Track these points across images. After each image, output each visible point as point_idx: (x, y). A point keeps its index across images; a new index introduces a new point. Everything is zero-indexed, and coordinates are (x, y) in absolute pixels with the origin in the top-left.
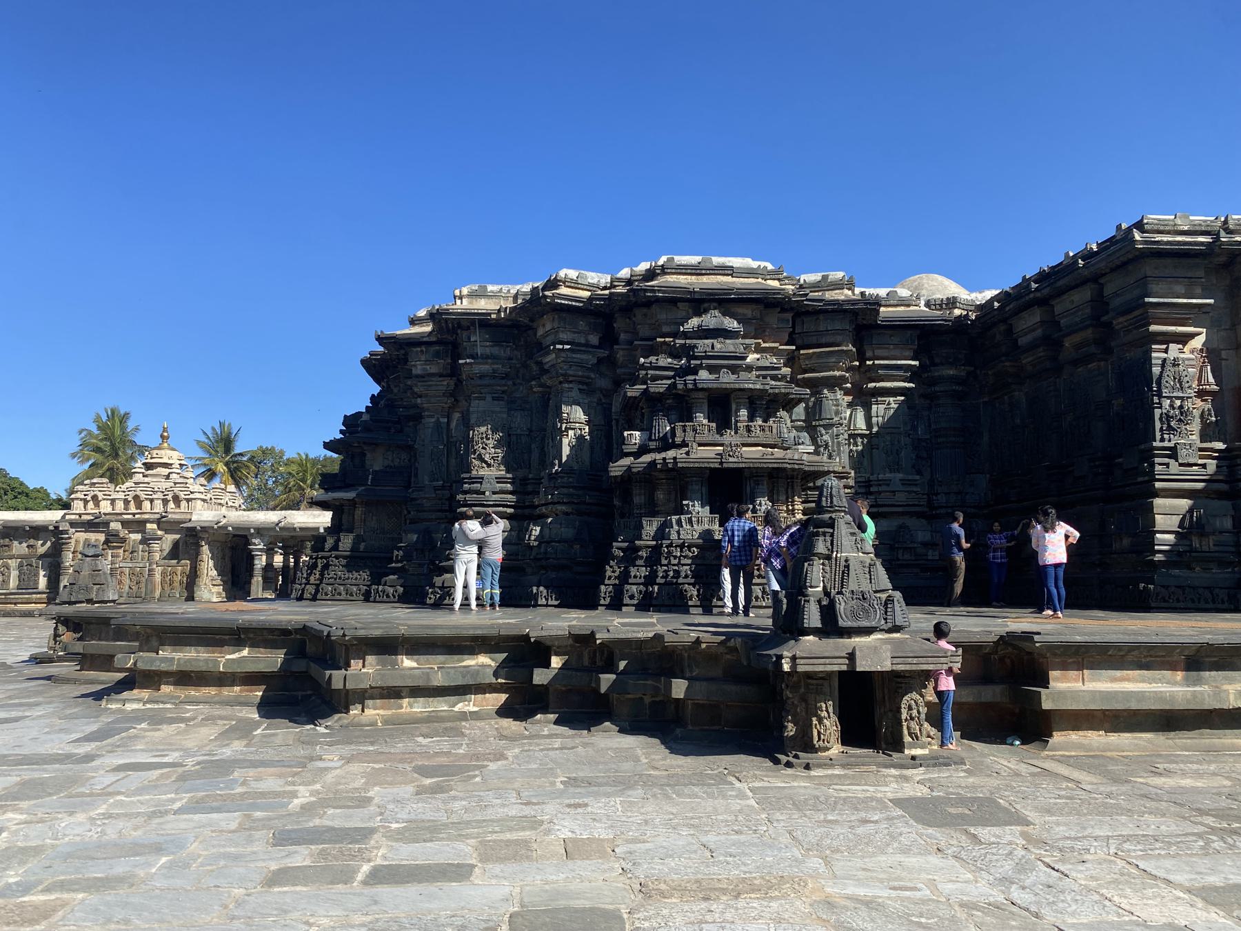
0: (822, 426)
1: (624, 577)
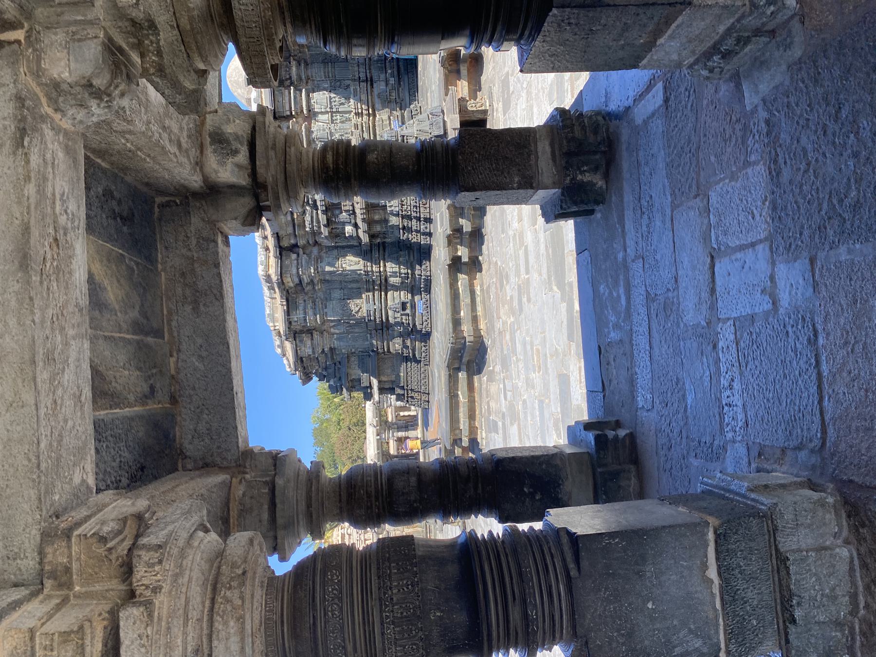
1: (417, 231)
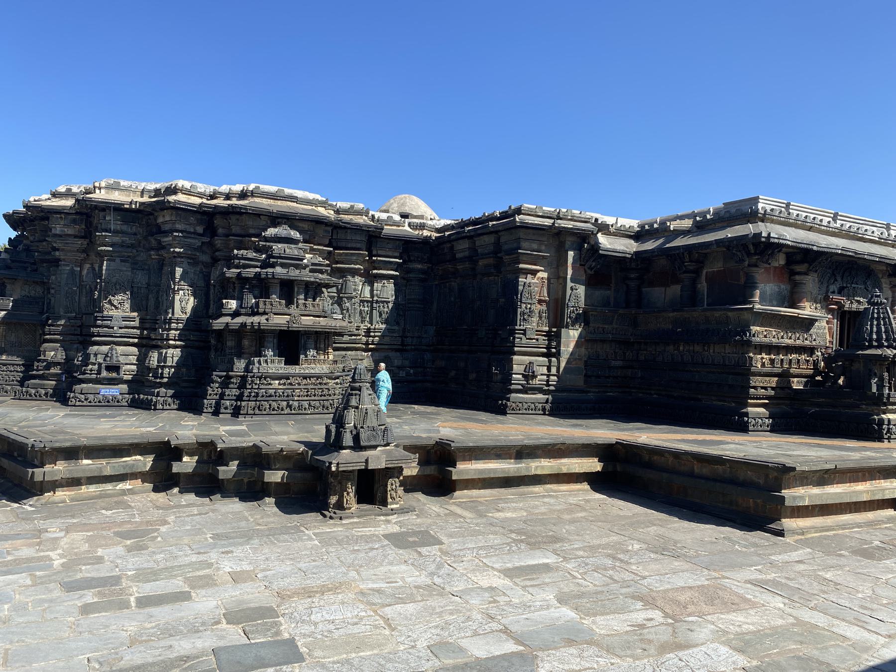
1: (222, 396)
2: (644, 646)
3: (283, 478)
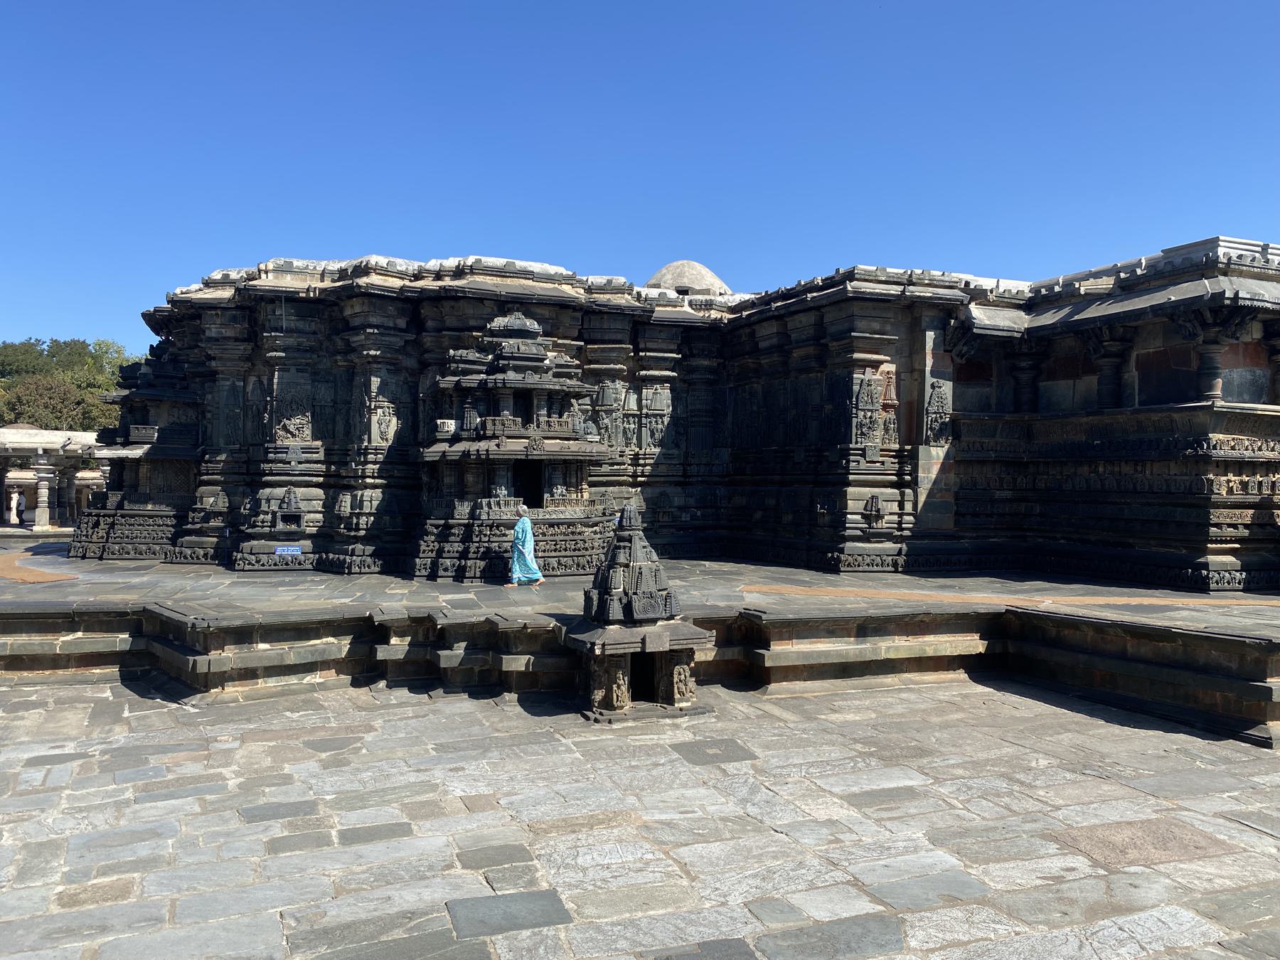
0: (605, 411)
1: (440, 553)
2: (1064, 908)
3: (527, 665)
